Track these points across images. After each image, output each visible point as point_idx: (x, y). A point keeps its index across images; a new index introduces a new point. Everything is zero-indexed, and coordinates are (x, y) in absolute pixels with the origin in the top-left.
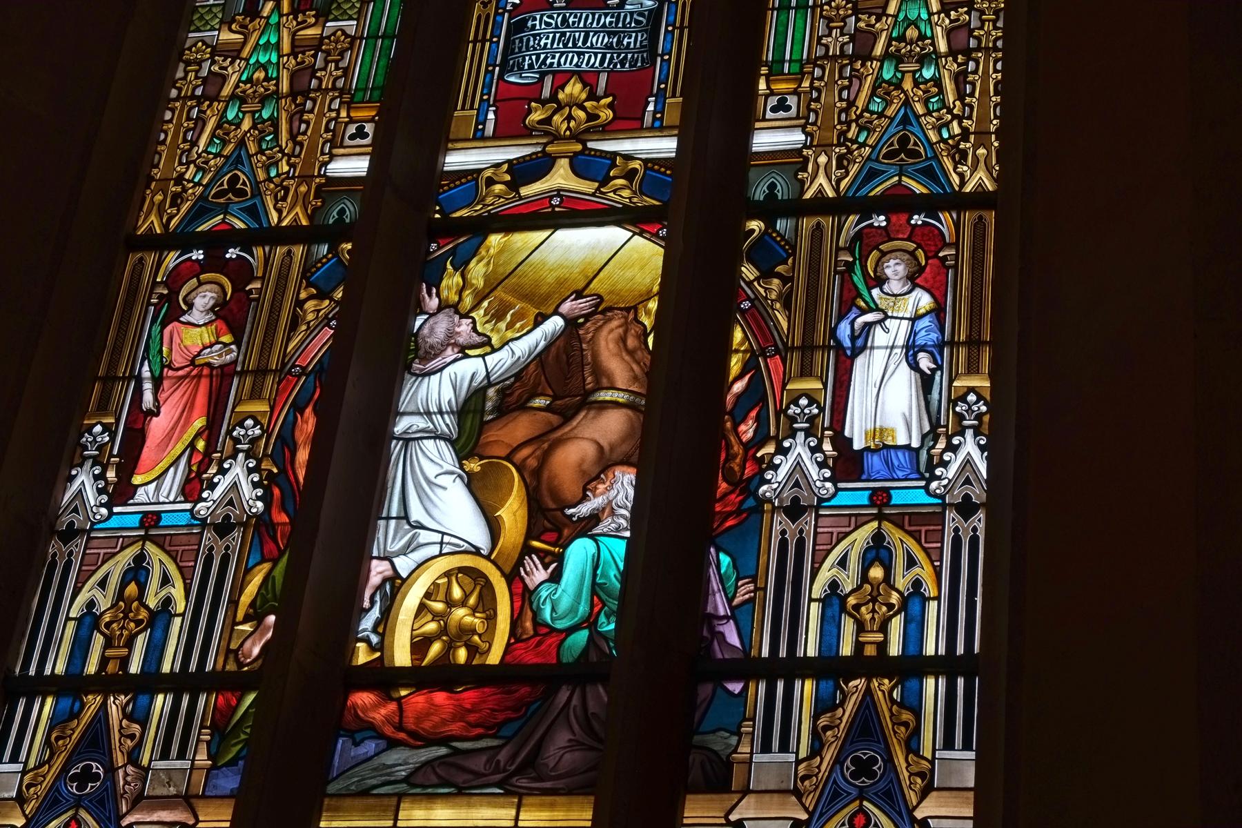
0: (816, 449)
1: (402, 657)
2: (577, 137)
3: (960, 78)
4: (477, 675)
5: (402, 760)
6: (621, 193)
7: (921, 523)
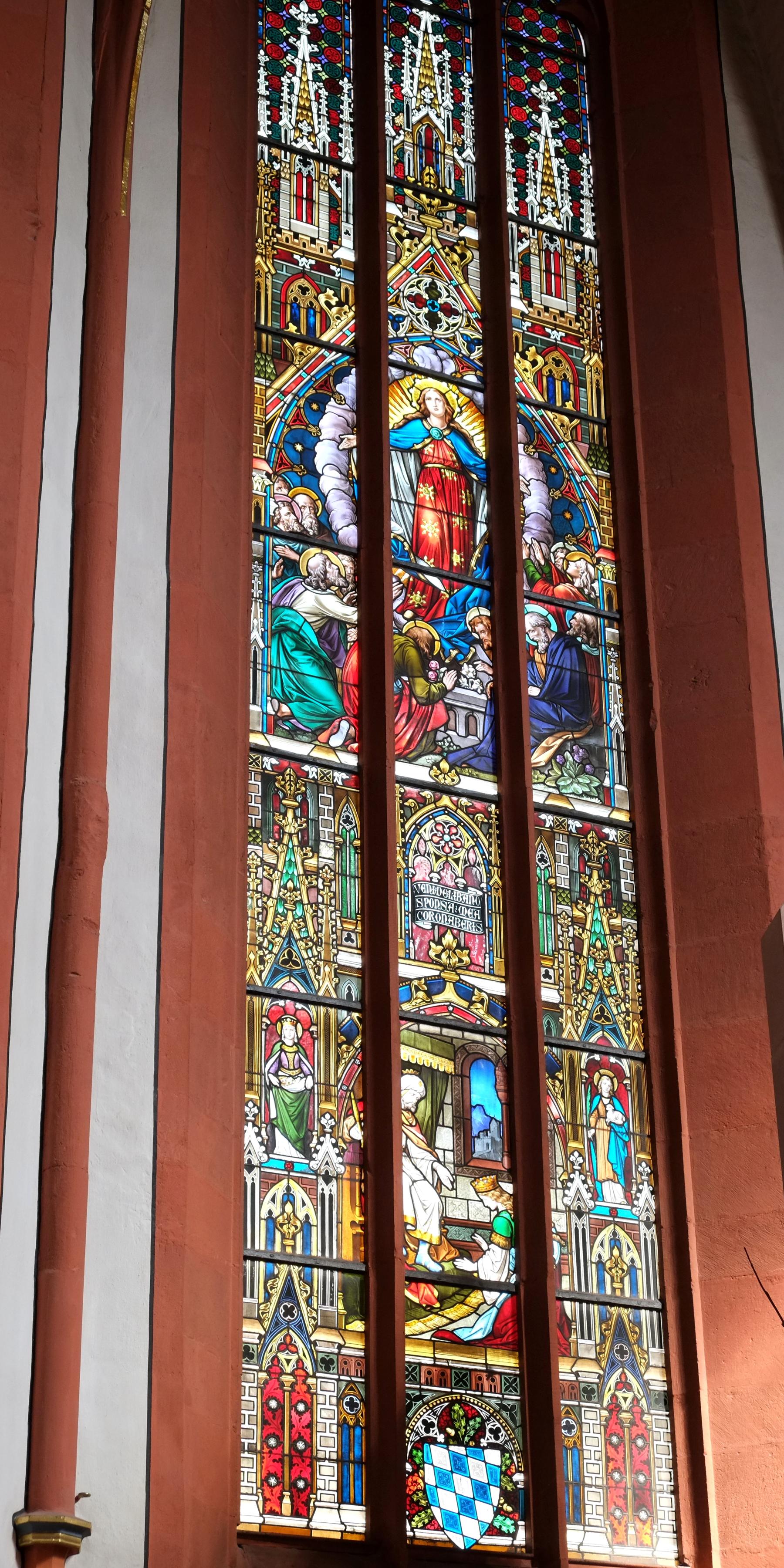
0: (584, 1182)
2: (454, 969)
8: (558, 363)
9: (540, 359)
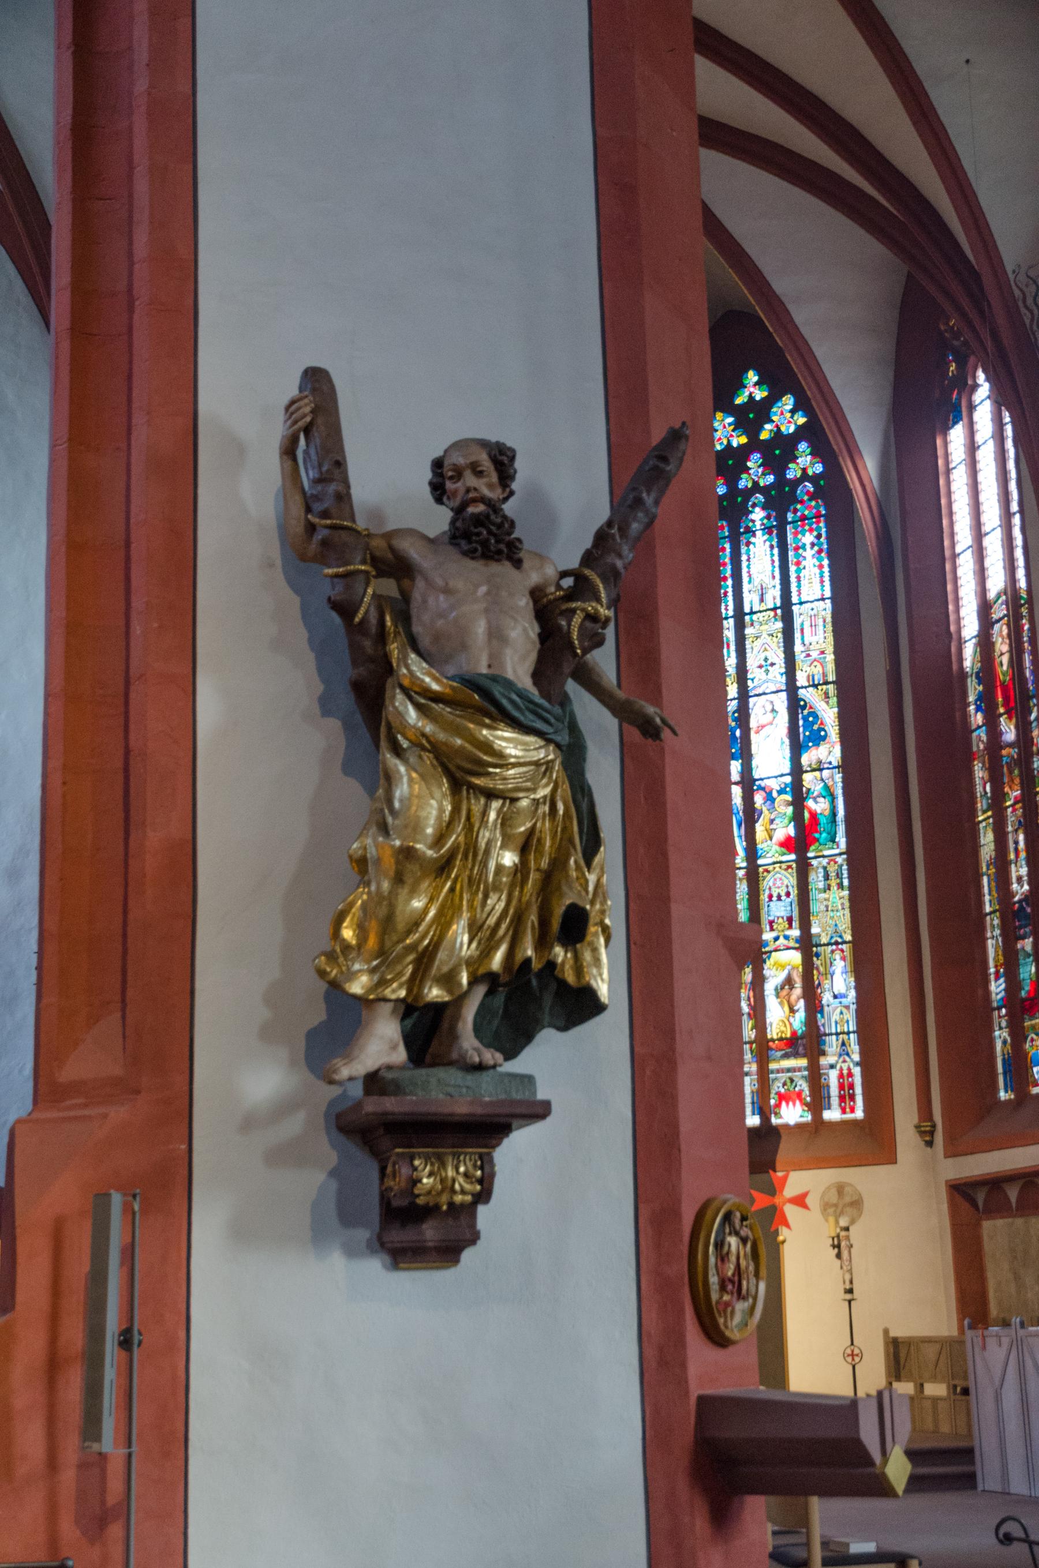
1: (775, 1037)
4: (786, 1039)
5: (779, 1054)
6: (792, 944)
7: (847, 1007)
9: (808, 669)
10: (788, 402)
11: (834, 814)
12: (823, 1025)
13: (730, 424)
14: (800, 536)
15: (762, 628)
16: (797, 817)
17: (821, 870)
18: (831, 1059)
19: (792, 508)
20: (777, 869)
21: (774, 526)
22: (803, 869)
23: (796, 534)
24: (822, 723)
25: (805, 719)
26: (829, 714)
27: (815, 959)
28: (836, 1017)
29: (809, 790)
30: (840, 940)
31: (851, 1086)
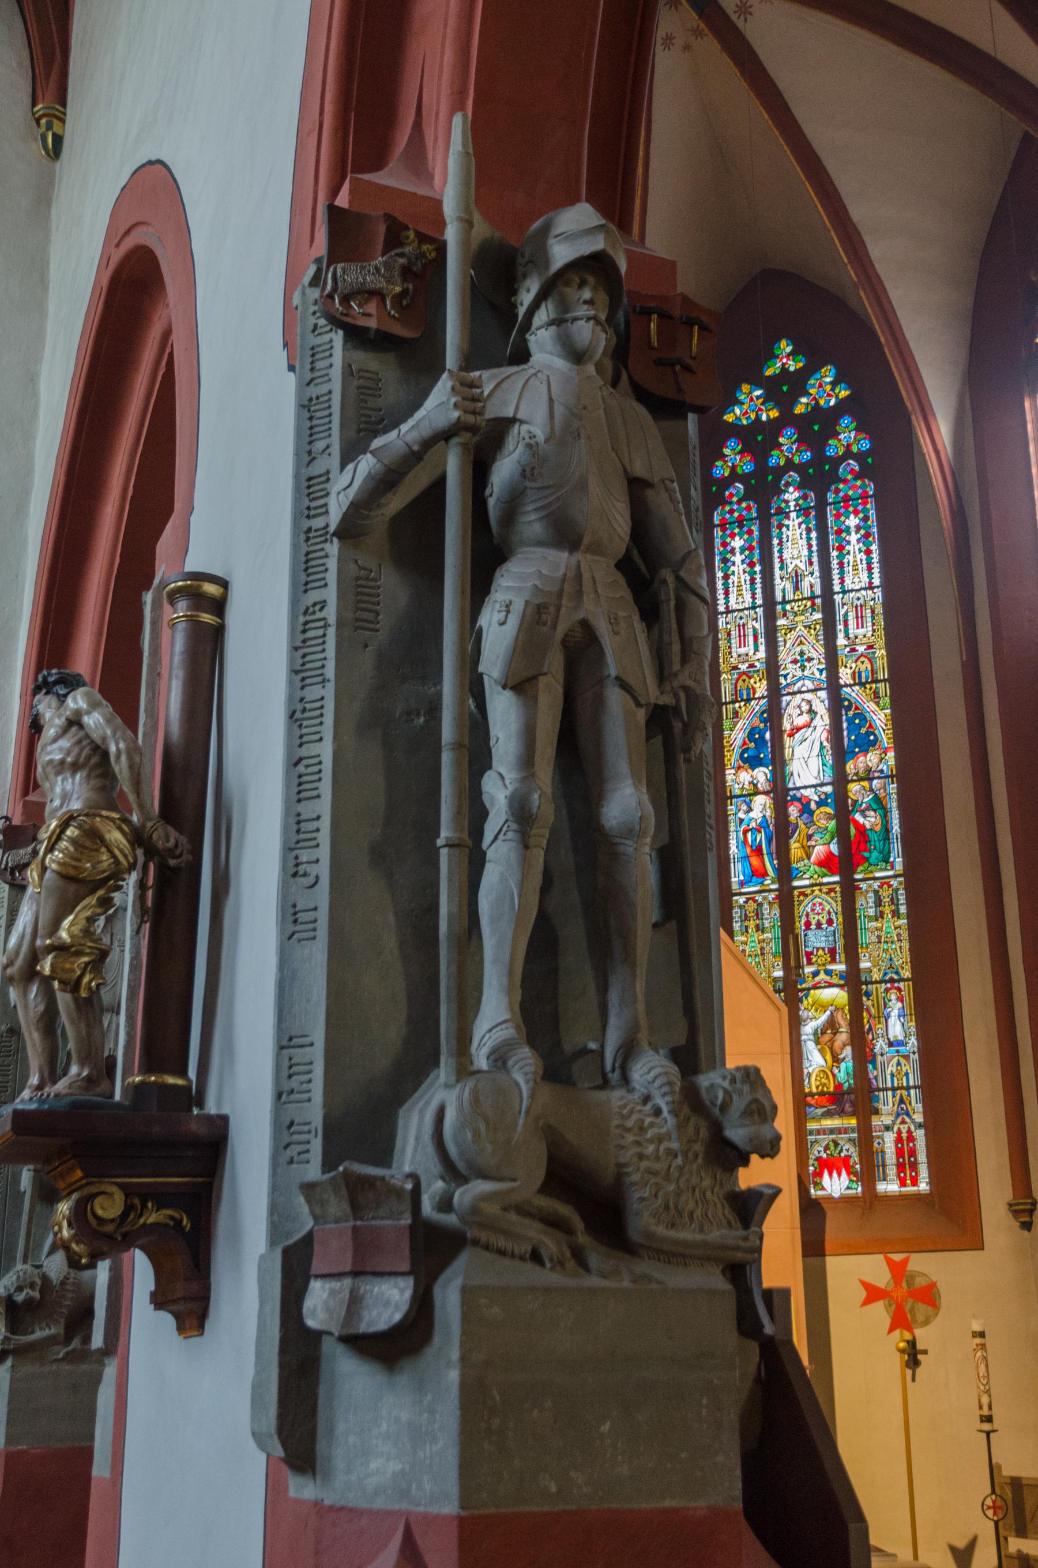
1: (814, 1090)
2: (824, 965)
3: (900, 947)
4: (829, 1093)
5: (820, 1111)
6: (835, 980)
7: (906, 1057)
8: (863, 663)
9: (854, 665)
10: (828, 375)
11: (887, 830)
12: (876, 1078)
13: (758, 397)
14: (843, 518)
15: (797, 619)
16: (841, 833)
17: (871, 894)
18: (887, 1120)
19: (833, 488)
20: (817, 892)
21: (812, 507)
22: (849, 892)
23: (838, 516)
24: (871, 726)
25: (850, 722)
26: (880, 717)
27: (864, 999)
28: (891, 1068)
29: (855, 802)
30: (896, 977)
31: (913, 1152)
